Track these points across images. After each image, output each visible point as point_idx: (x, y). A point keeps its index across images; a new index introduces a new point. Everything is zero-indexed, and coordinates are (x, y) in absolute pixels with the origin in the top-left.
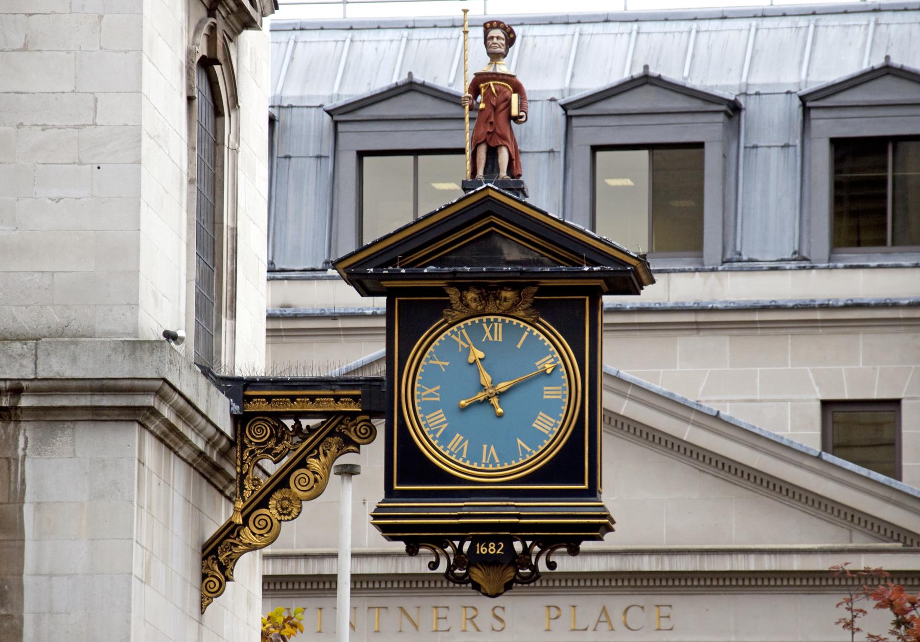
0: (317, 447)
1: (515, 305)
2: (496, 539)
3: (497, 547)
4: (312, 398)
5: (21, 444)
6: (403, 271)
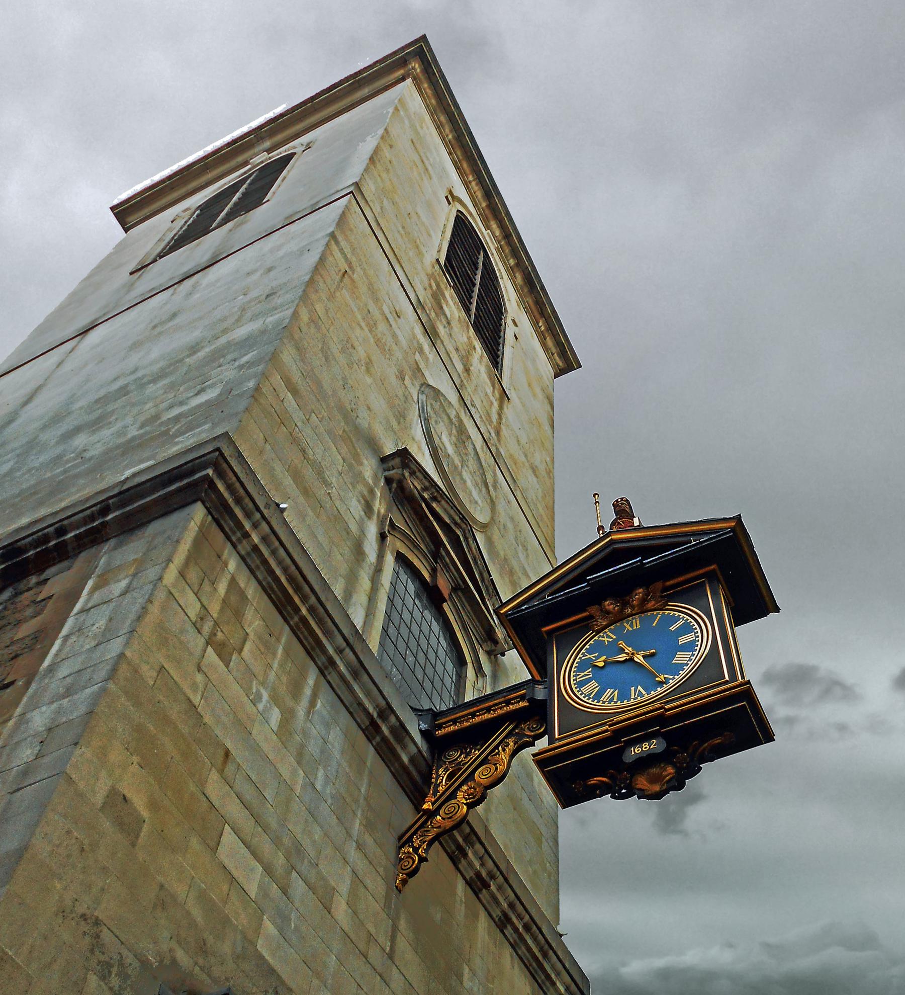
0: (497, 747)
1: (644, 601)
2: (647, 738)
4: (488, 710)
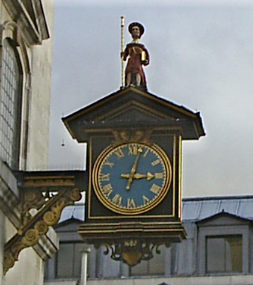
0: (55, 202)
1: (142, 139)
2: (134, 239)
3: (134, 243)
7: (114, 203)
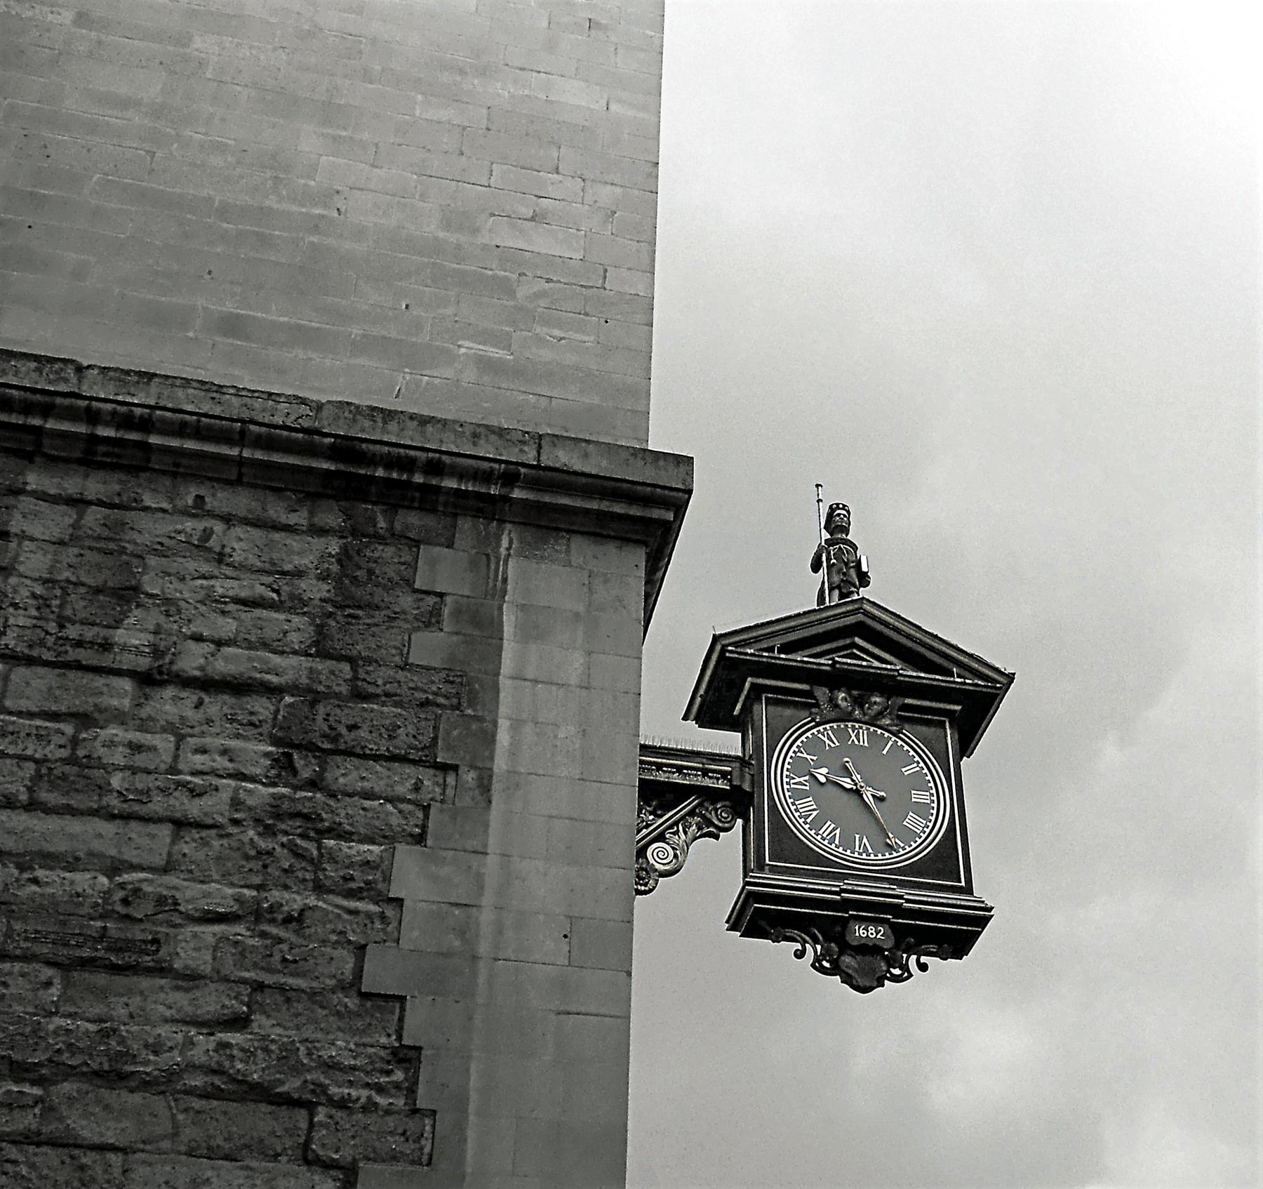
0: (676, 824)
1: (880, 714)
4: (680, 769)
5: (505, 543)
6: (783, 656)
7: (824, 838)
